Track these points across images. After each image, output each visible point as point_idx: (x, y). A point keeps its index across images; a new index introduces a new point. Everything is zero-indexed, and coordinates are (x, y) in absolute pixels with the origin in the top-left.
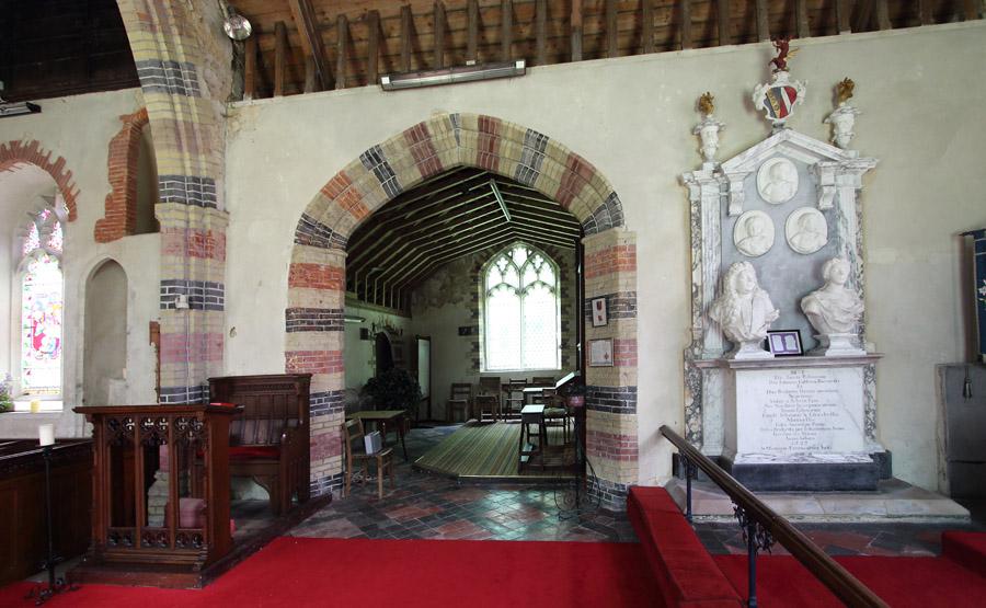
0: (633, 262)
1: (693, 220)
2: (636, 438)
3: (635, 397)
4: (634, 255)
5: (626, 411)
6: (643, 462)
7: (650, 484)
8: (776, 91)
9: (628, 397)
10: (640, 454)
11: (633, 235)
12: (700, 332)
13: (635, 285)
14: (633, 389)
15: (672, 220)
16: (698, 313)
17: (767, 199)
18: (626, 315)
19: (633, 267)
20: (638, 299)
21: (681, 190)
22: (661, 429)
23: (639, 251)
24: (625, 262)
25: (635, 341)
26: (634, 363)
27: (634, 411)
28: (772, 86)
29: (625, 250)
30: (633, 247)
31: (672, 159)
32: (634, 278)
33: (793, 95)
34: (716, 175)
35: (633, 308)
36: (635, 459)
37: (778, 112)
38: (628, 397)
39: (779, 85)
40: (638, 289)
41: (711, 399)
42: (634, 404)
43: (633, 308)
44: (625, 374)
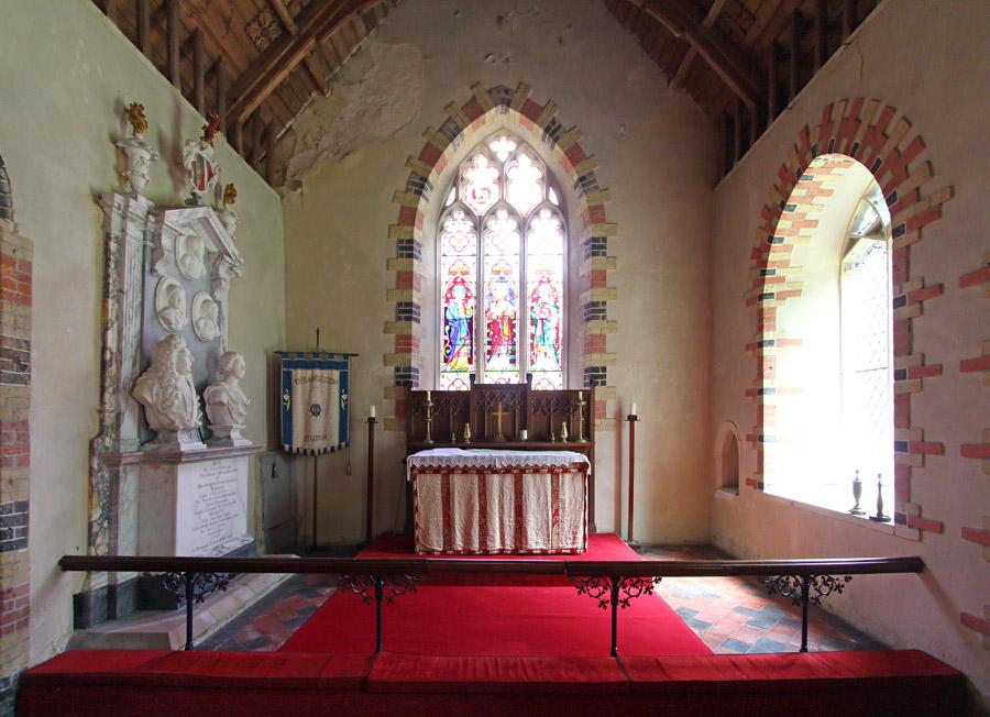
0: (27, 289)
1: (108, 258)
2: (26, 588)
3: (26, 519)
4: (28, 279)
5: (12, 547)
6: (36, 623)
7: (46, 657)
8: (200, 158)
9: (16, 520)
10: (31, 613)
11: (26, 245)
12: (114, 415)
13: (28, 330)
14: (24, 506)
15: (83, 251)
16: (111, 389)
17: (183, 270)
18: (14, 379)
19: (26, 300)
20: (34, 354)
21: (93, 209)
22: (61, 563)
23: (36, 274)
24: (13, 286)
25: (25, 424)
26: (25, 462)
27: (24, 543)
28: (200, 153)
29: (13, 265)
30: (29, 266)
31: (90, 167)
32: (28, 317)
33: (211, 175)
34: (151, 218)
35: (24, 368)
36: (25, 624)
37: (199, 182)
38: (16, 520)
39: (204, 156)
40: (33, 339)
41: (126, 505)
42: (25, 532)
43: (24, 368)
44: (11, 482)
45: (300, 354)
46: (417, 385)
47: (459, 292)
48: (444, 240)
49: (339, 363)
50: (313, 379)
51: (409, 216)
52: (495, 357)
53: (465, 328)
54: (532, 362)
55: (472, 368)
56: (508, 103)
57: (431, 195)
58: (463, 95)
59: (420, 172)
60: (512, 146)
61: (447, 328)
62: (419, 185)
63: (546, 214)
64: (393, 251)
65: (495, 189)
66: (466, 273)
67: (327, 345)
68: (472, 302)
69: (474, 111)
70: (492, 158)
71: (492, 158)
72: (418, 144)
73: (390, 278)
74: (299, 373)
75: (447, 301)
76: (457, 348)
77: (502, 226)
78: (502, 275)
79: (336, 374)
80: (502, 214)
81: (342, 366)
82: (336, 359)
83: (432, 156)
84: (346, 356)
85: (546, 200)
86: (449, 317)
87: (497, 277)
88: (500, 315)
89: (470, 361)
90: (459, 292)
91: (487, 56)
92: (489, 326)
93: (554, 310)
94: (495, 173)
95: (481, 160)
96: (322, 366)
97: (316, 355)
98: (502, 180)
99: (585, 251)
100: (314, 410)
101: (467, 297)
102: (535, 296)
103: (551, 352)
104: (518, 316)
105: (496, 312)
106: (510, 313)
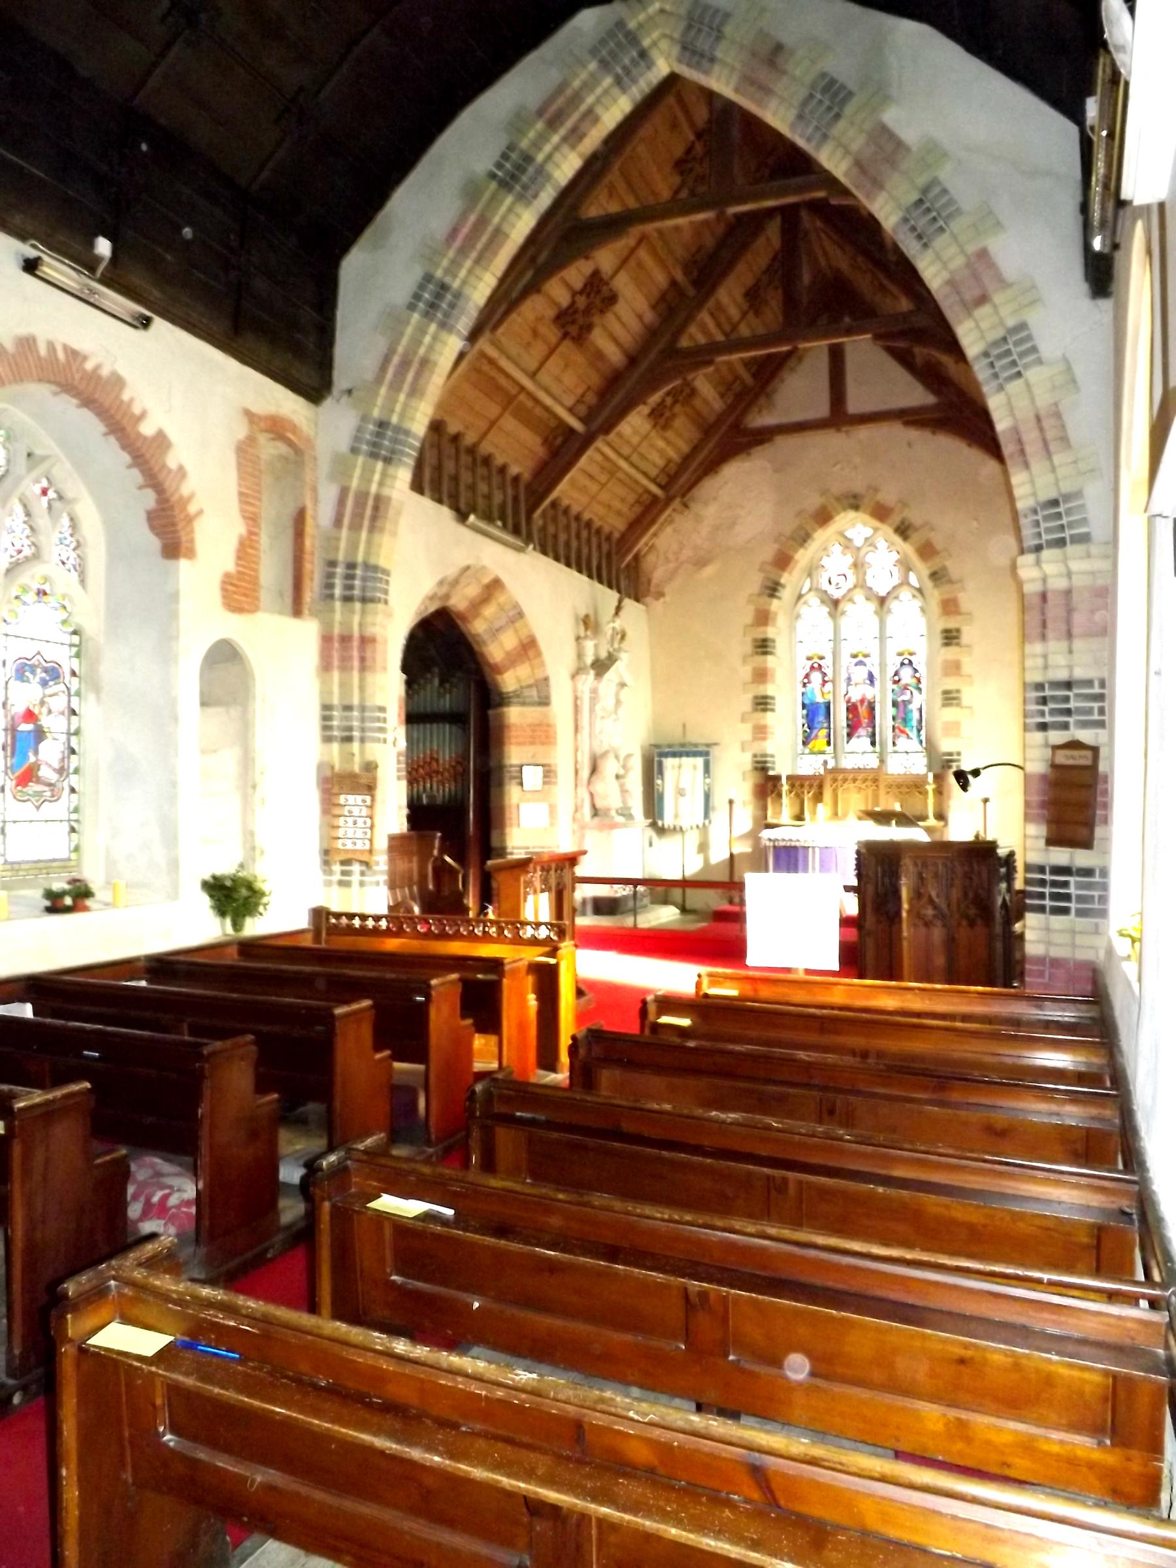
45: (670, 746)
46: (773, 769)
47: (816, 677)
48: (800, 624)
49: (702, 752)
50: (680, 767)
51: (763, 618)
52: (854, 740)
53: (822, 710)
54: (894, 744)
55: (830, 749)
56: (856, 508)
57: (786, 594)
58: (813, 501)
59: (773, 576)
60: (869, 532)
61: (805, 712)
62: (773, 589)
63: (905, 594)
64: (748, 648)
65: (850, 574)
66: (822, 658)
67: (693, 737)
68: (829, 686)
69: (823, 517)
70: (847, 544)
71: (847, 544)
72: (768, 552)
73: (746, 672)
74: (669, 762)
75: (804, 685)
76: (815, 732)
77: (860, 612)
78: (860, 658)
79: (700, 761)
80: (859, 596)
81: (706, 754)
82: (701, 749)
83: (783, 561)
84: (708, 745)
85: (905, 582)
86: (807, 702)
87: (856, 660)
88: (859, 698)
89: (829, 743)
90: (816, 677)
91: (835, 465)
92: (848, 709)
93: (915, 692)
94: (849, 559)
95: (837, 549)
96: (688, 754)
97: (683, 745)
98: (857, 566)
99: (938, 640)
100: (681, 793)
101: (824, 682)
102: (896, 678)
103: (913, 734)
104: (877, 700)
105: (855, 697)
106: (869, 697)
